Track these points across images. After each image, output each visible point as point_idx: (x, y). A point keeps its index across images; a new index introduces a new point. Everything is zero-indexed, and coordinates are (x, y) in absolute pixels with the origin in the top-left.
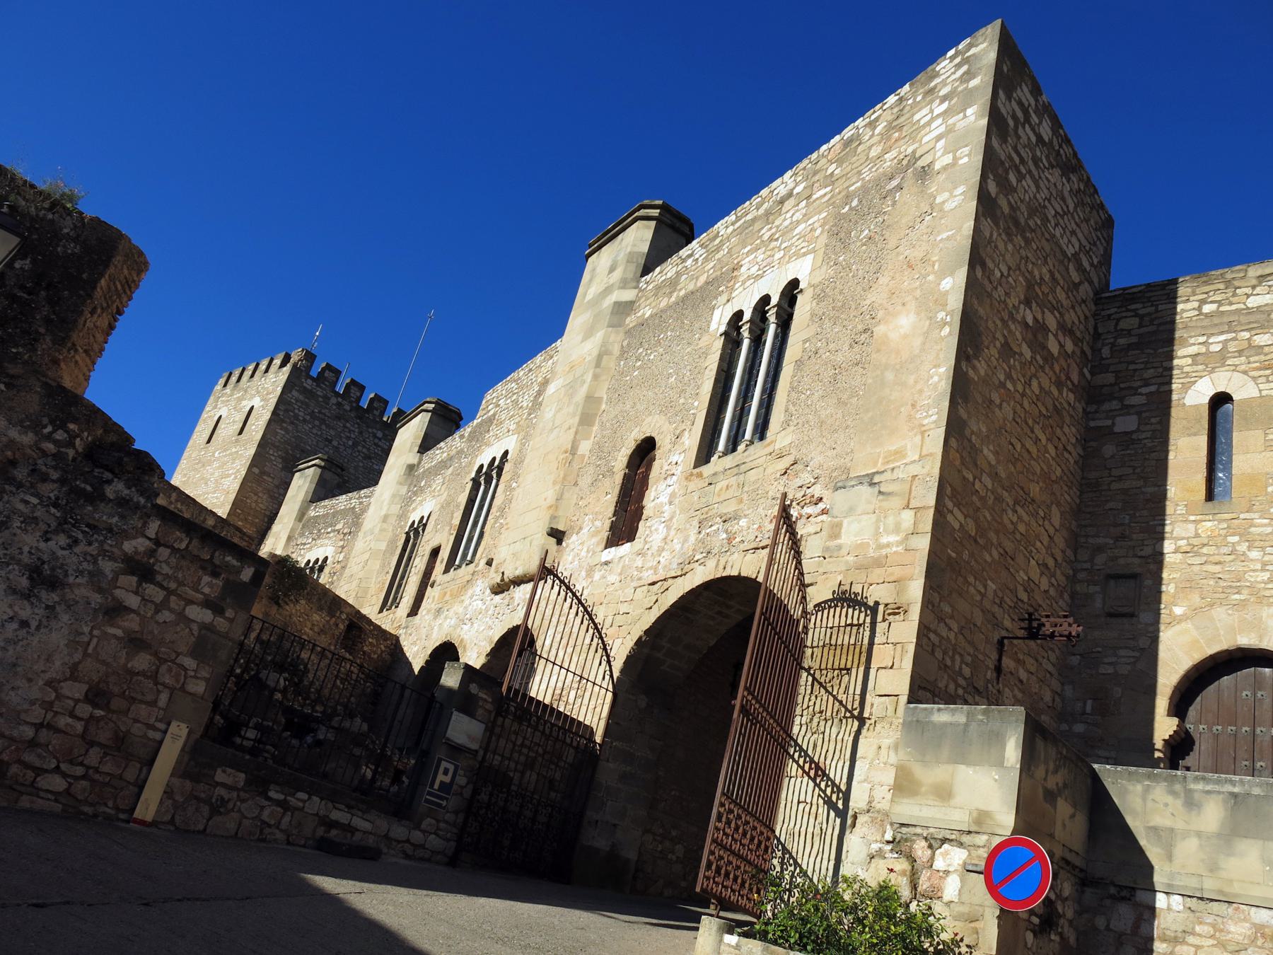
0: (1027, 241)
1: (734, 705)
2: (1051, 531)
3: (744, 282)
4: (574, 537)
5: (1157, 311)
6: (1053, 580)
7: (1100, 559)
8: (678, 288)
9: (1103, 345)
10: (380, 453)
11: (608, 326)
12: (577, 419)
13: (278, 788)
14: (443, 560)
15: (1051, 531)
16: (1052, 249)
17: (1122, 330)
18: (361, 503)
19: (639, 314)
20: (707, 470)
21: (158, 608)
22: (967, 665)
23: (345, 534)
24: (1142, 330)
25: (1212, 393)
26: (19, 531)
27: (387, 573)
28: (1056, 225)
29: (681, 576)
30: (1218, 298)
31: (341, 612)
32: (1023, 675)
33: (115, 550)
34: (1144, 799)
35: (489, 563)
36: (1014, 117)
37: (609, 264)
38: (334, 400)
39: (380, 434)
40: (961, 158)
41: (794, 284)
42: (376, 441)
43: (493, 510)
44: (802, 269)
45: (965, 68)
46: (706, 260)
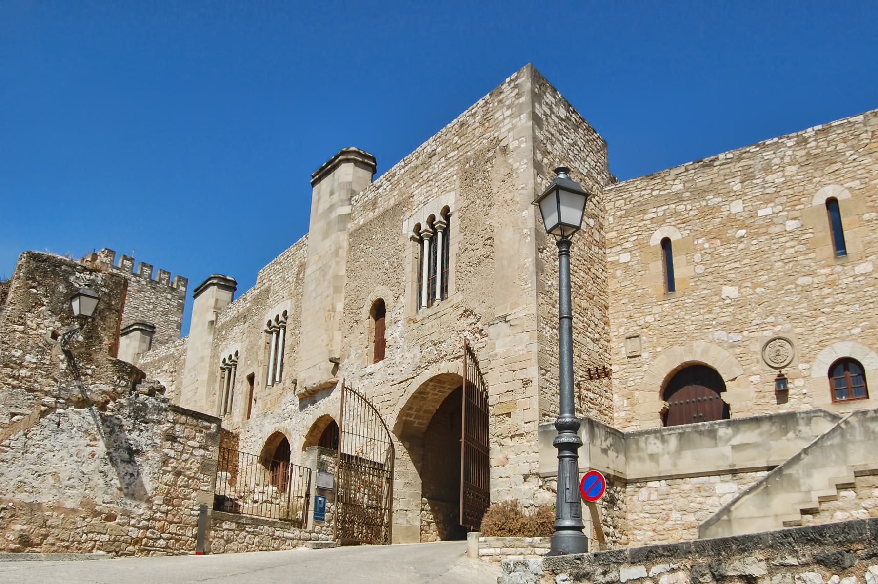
1: (461, 442)
4: (346, 360)
11: (339, 231)
25: (661, 238)
27: (214, 394)
30: (658, 187)
34: (646, 443)
37: (329, 189)
39: (169, 296)
44: (450, 200)
45: (516, 91)
46: (392, 190)
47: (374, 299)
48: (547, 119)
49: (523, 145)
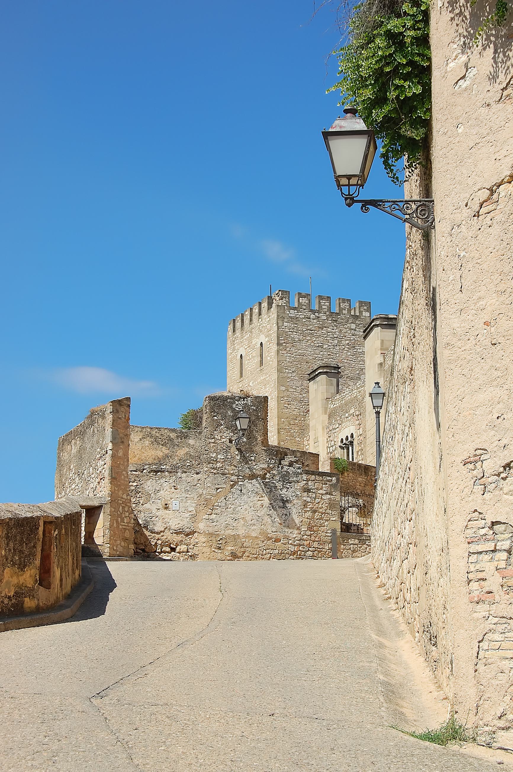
18: (360, 392)
21: (315, 498)
26: (275, 491)
31: (371, 472)
39: (353, 326)
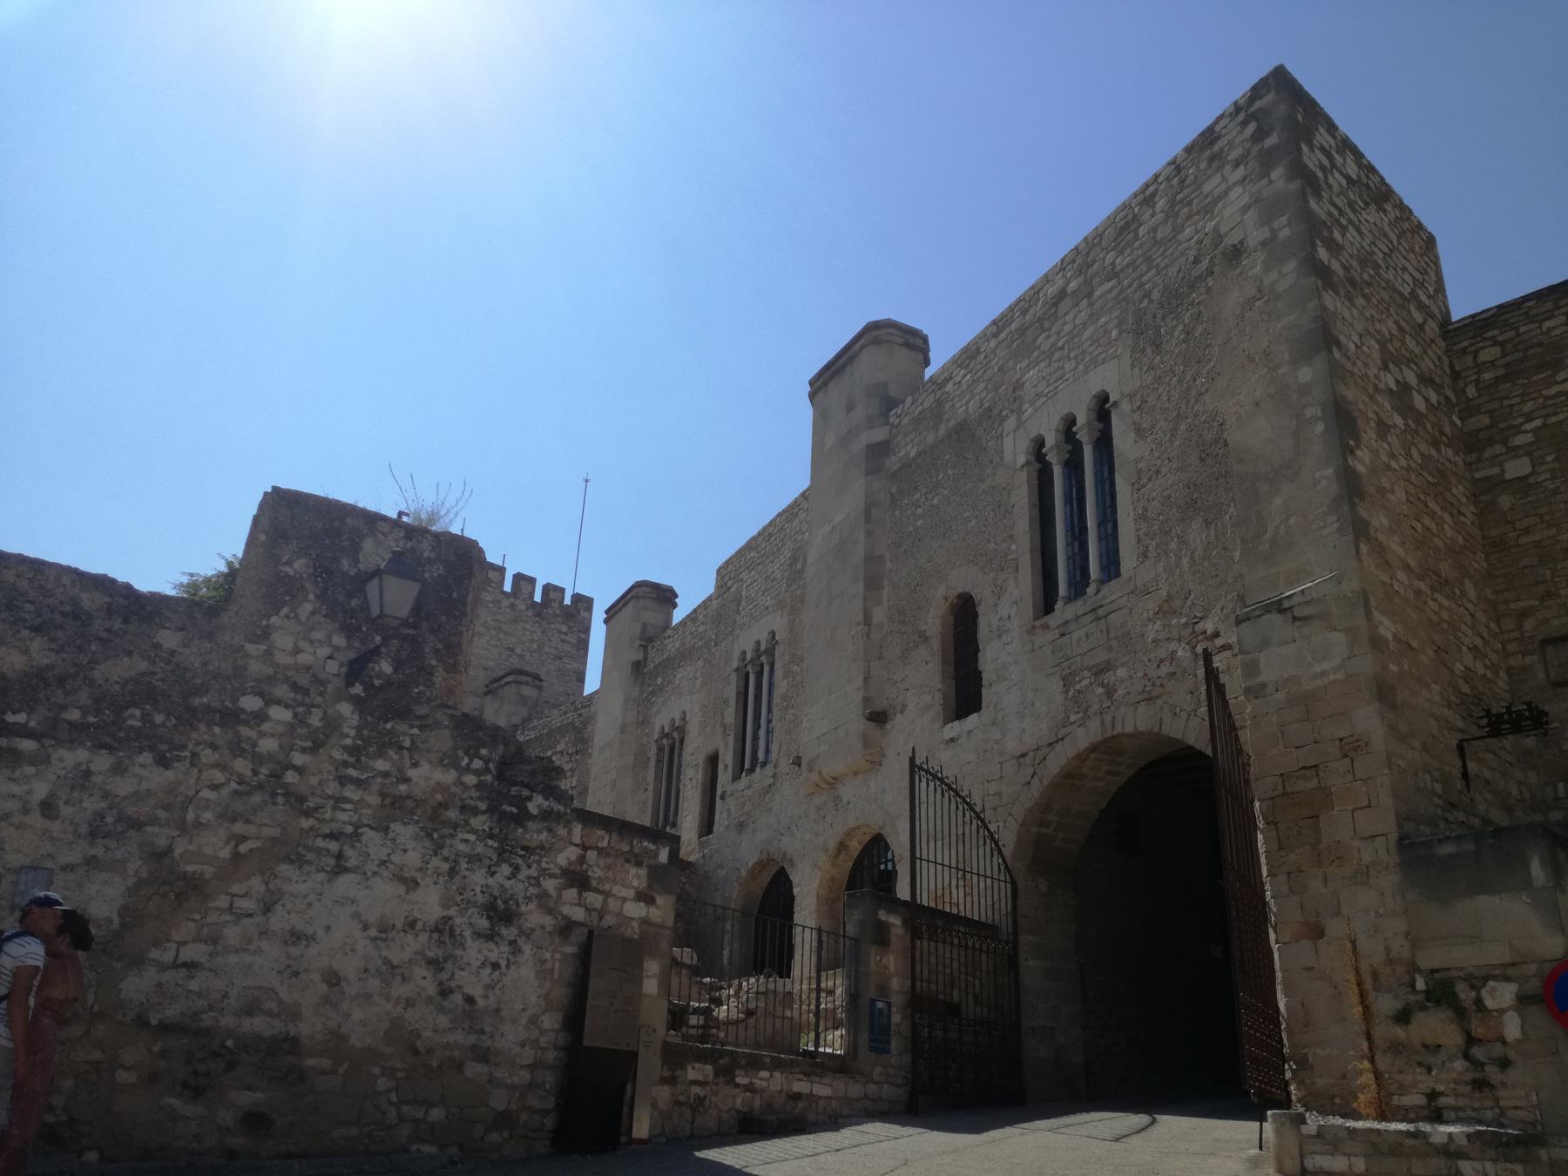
0: (1366, 297)
2: (1471, 608)
3: (1032, 403)
4: (899, 718)
5: (1518, 335)
6: (1488, 662)
7: (1528, 625)
8: (945, 418)
9: (1466, 385)
10: (569, 649)
11: (867, 474)
12: (861, 585)
13: (742, 1073)
14: (726, 766)
15: (1471, 608)
16: (1391, 297)
17: (1484, 363)
18: (580, 715)
19: (902, 453)
20: (1054, 619)
22: (1437, 781)
23: (571, 755)
24: (1508, 359)
26: (467, 873)
27: (646, 790)
28: (1387, 268)
29: (1057, 742)
32: (1487, 774)
33: (551, 866)
35: (798, 762)
36: (1322, 168)
38: (505, 603)
39: (564, 629)
40: (1280, 230)
41: (1103, 398)
42: (563, 637)
43: (776, 700)
44: (1109, 377)
45: (1252, 127)
47: (953, 594)
48: (1326, 177)
49: (1285, 233)
